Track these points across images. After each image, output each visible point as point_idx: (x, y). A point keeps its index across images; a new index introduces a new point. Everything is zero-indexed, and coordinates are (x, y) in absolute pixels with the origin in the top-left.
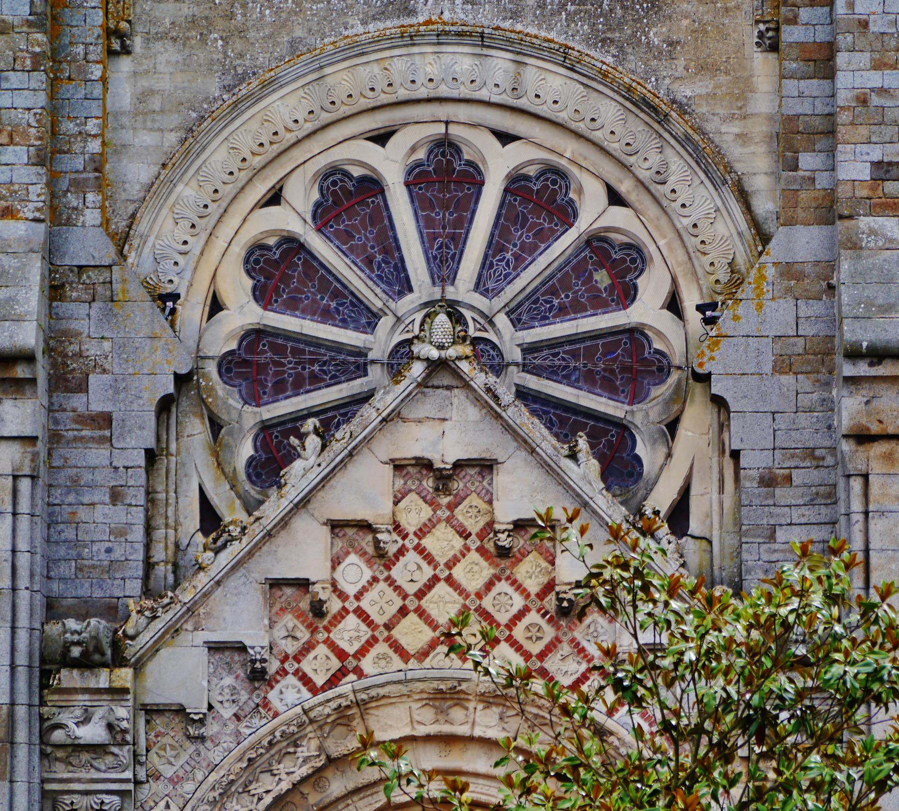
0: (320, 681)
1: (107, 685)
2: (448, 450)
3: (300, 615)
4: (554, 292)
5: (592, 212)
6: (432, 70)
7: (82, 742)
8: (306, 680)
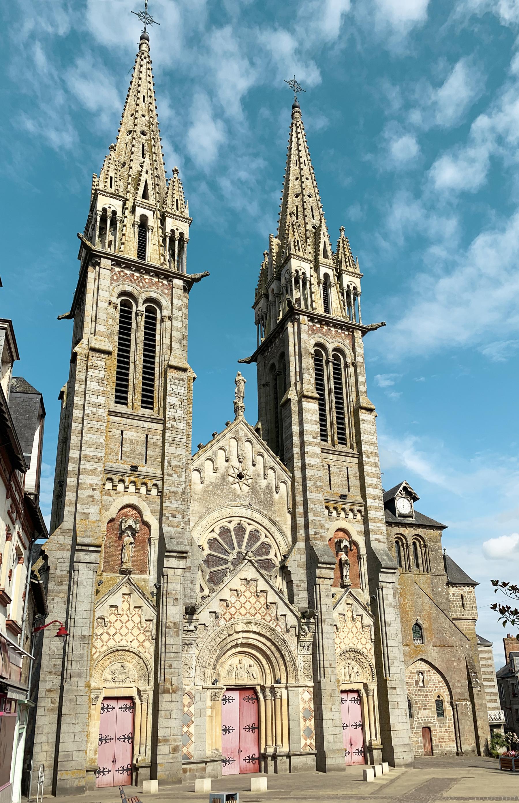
0: (228, 619)
2: (249, 577)
3: (224, 607)
4: (256, 552)
5: (263, 539)
6: (239, 511)
8: (225, 619)
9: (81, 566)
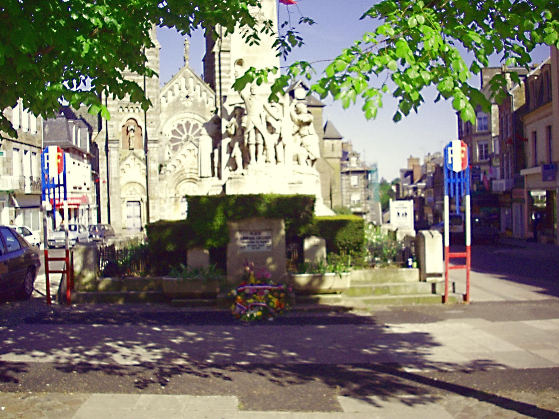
9: (112, 149)
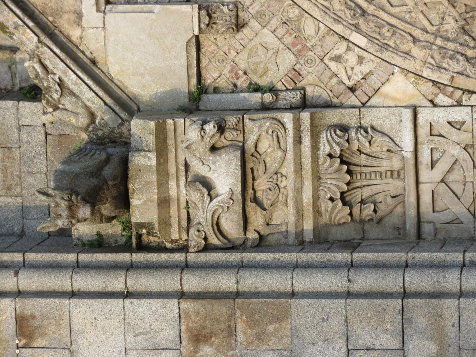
1: (153, 156)
7: (238, 189)
